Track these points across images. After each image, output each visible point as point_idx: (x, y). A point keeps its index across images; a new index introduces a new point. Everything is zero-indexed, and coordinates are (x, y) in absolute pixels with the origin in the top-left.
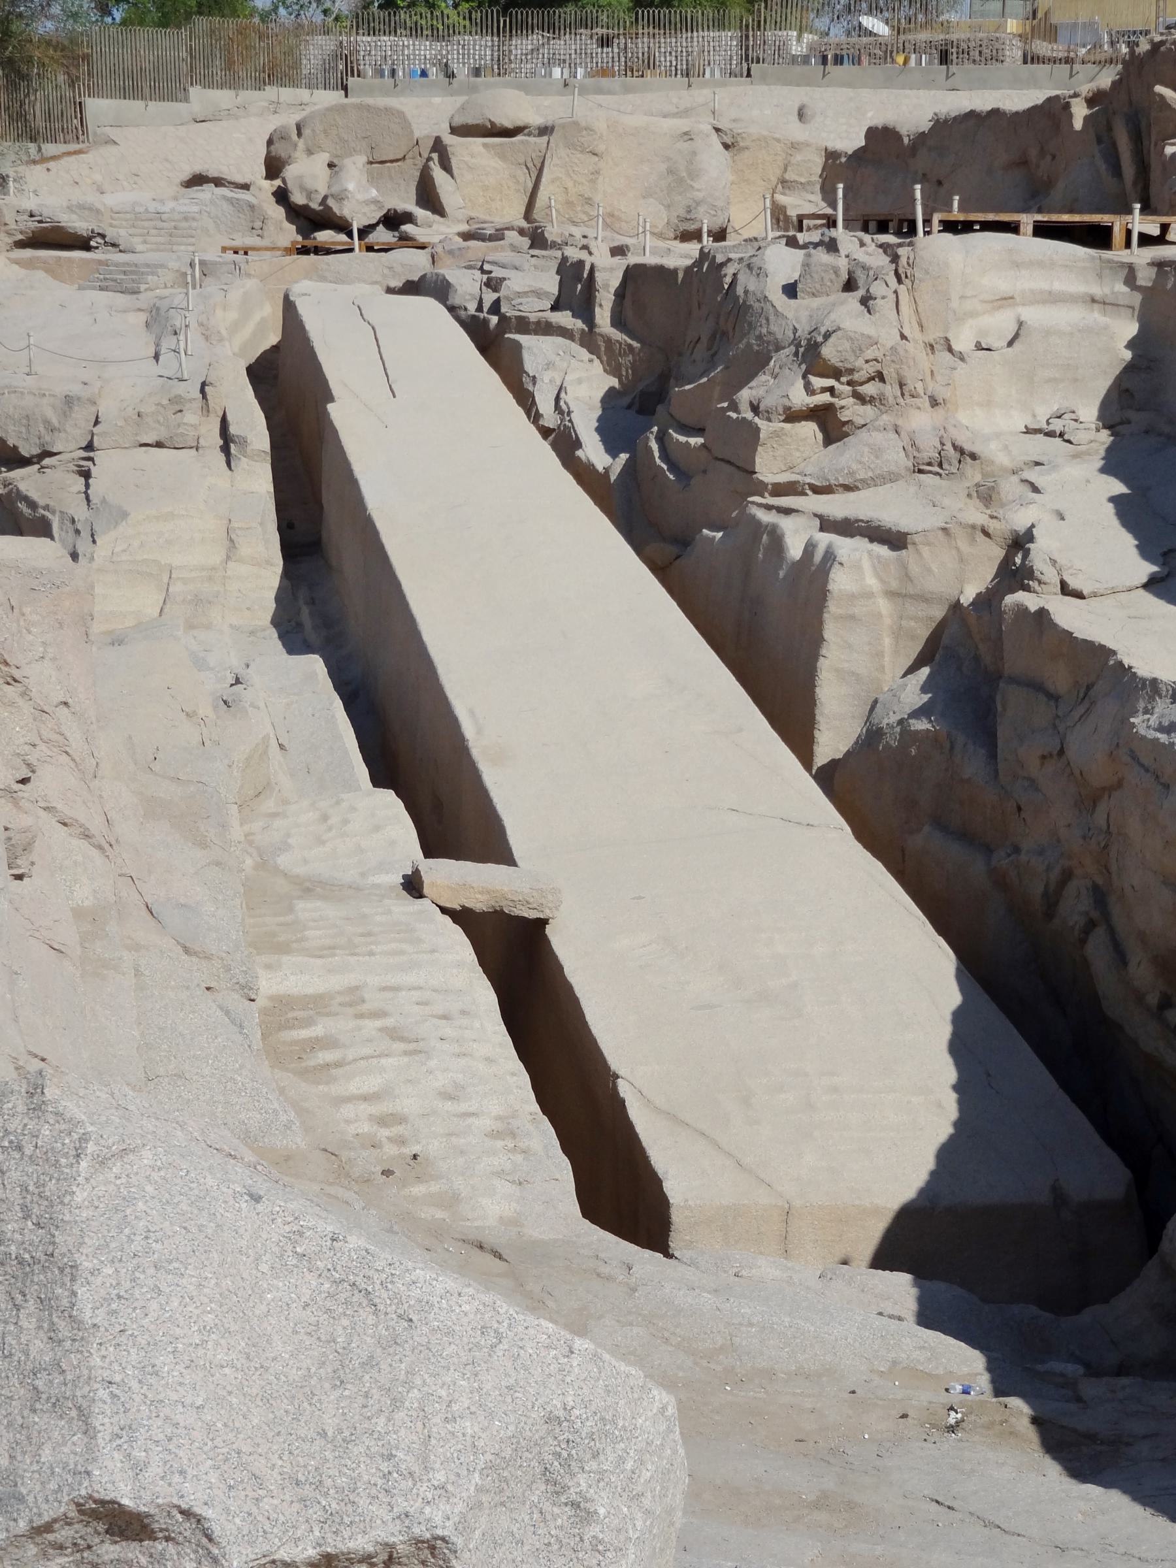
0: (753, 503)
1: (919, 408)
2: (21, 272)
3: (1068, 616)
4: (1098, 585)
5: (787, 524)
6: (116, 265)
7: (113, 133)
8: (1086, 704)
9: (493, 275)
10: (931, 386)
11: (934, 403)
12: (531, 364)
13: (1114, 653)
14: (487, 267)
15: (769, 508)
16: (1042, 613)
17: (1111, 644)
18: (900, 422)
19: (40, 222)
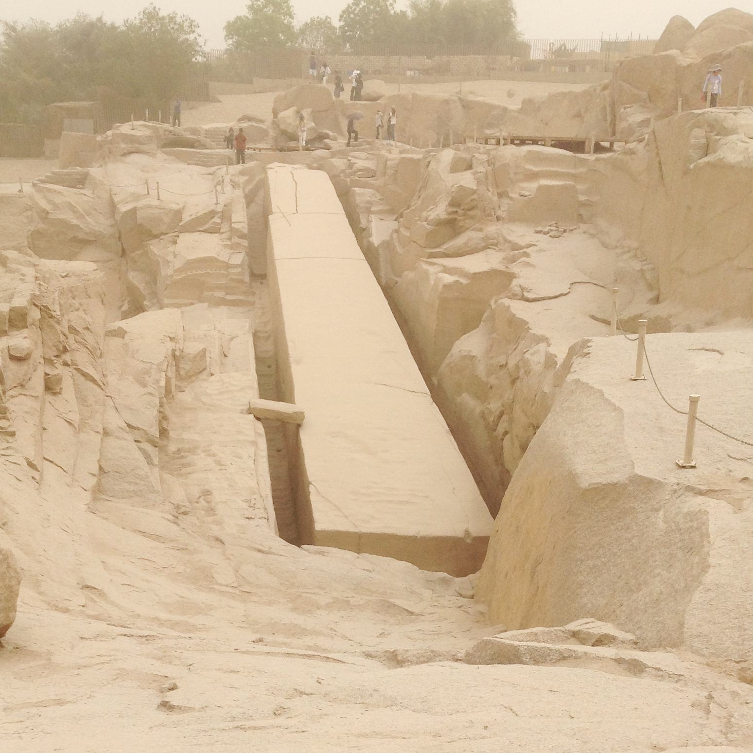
0: (423, 261)
1: (491, 221)
2: (166, 157)
3: (519, 309)
4: (537, 296)
5: (432, 269)
6: (204, 154)
7: (221, 98)
8: (517, 344)
9: (351, 161)
10: (499, 213)
11: (498, 219)
12: (358, 200)
13: (528, 323)
14: (349, 158)
15: (427, 262)
16: (509, 307)
17: (527, 320)
18: (482, 226)
19: (174, 135)
